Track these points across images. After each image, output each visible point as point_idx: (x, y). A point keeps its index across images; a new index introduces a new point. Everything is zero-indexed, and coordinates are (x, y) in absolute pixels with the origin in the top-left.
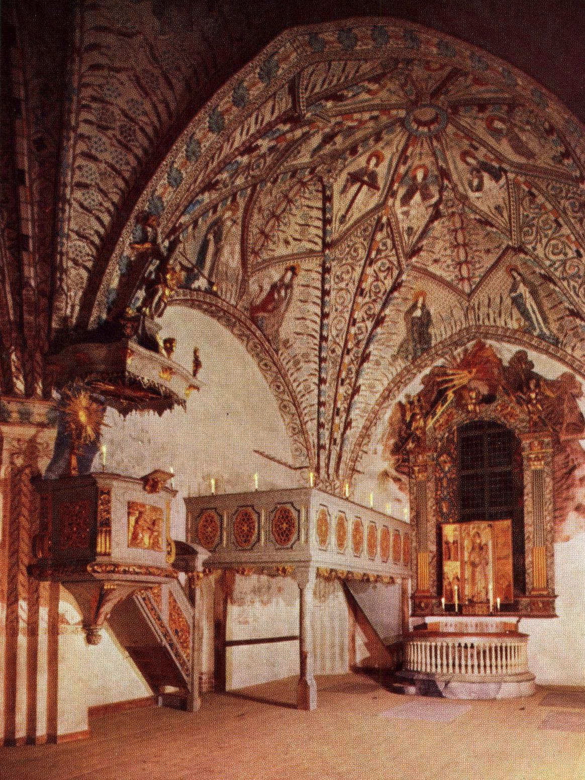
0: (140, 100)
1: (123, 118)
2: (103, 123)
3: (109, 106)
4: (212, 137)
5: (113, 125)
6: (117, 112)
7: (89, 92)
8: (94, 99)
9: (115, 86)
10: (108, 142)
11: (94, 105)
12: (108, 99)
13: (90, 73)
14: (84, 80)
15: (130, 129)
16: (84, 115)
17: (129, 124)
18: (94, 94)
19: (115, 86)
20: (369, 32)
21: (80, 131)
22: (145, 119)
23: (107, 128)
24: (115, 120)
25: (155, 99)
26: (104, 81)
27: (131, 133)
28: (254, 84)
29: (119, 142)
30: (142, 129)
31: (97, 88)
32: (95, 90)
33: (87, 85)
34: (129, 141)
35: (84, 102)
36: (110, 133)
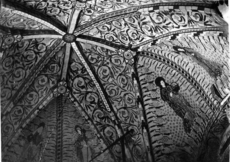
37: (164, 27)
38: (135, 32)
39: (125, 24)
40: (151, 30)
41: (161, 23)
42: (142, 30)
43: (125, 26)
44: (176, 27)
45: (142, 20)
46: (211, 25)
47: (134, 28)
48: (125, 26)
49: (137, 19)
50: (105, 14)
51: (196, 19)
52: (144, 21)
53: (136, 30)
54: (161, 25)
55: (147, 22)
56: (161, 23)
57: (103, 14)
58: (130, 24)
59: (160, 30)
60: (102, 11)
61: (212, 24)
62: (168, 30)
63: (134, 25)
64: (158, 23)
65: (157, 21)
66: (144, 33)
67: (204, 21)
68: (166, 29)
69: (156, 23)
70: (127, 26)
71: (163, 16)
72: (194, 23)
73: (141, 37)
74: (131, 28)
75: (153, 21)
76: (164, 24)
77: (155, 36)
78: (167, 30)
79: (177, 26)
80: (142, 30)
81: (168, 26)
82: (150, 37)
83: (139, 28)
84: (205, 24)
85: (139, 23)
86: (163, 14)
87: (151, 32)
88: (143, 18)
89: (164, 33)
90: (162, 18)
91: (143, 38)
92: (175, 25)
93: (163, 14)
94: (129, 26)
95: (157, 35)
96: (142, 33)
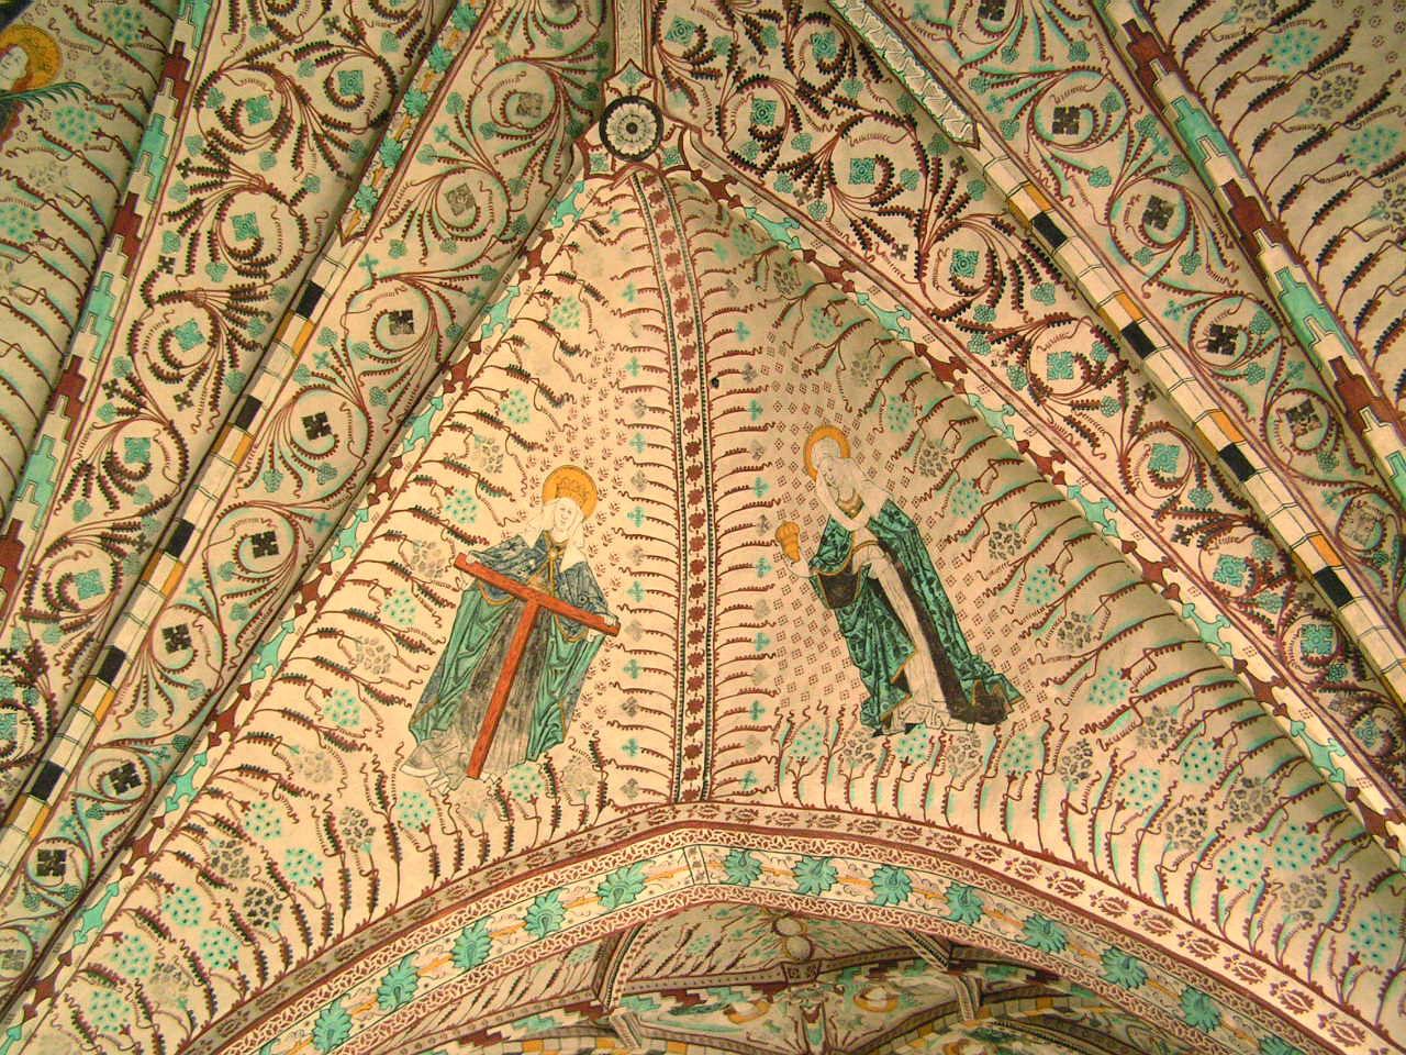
0: (318, 856)
1: (267, 878)
2: (216, 872)
3: (245, 846)
4: (452, 973)
5: (235, 883)
6: (256, 860)
7: (217, 807)
8: (219, 822)
9: (276, 815)
10: (208, 908)
11: (215, 833)
12: (249, 832)
13: (237, 773)
14: (217, 784)
15: (269, 901)
16: (184, 843)
17: (272, 888)
18: (226, 814)
19: (276, 815)
20: (869, 873)
21: (156, 868)
22: (315, 894)
23: (218, 883)
24: (245, 874)
25: (351, 864)
26: (259, 800)
27: (270, 909)
28: (581, 901)
29: (235, 918)
30: (297, 909)
31: (237, 808)
32: (230, 807)
33: (216, 794)
34: (258, 923)
35: (194, 820)
36: (221, 894)
37: (196, 209)
38: (288, 22)
39: (356, 36)
40: (231, 123)
41: (220, 216)
42: (269, 69)
43: (354, 20)
44: (153, 277)
45: (303, 128)
46: (66, 498)
47: (308, 39)
48: (354, 20)
49: (325, 120)
50: (483, 33)
51: (128, 441)
52: (293, 137)
53: (290, 39)
54: (211, 199)
55: (275, 148)
56: (220, 216)
57: (490, 25)
58: (340, 54)
59: (201, 171)
60: (502, 37)
61: (68, 508)
62: (173, 216)
63: (319, 62)
64: (228, 199)
65: (243, 204)
66: (252, 61)
67: (100, 478)
68: (184, 211)
69: (238, 190)
70: (344, 24)
71: (241, 272)
72: (121, 412)
73: (249, 23)
74: (318, 34)
75: (259, 186)
76: (205, 224)
77: (198, 107)
78: (176, 207)
79: (157, 291)
80: (269, 69)
81: (185, 241)
82: (214, 77)
83: (288, 67)
84: (85, 468)
85: (303, 99)
86: (247, 281)
87: (228, 111)
88: (306, 158)
89: (176, 175)
90: (233, 253)
91: (234, 28)
92: (164, 284)
93: (247, 281)
94: (336, 39)
95: (192, 129)
96: (257, 53)
